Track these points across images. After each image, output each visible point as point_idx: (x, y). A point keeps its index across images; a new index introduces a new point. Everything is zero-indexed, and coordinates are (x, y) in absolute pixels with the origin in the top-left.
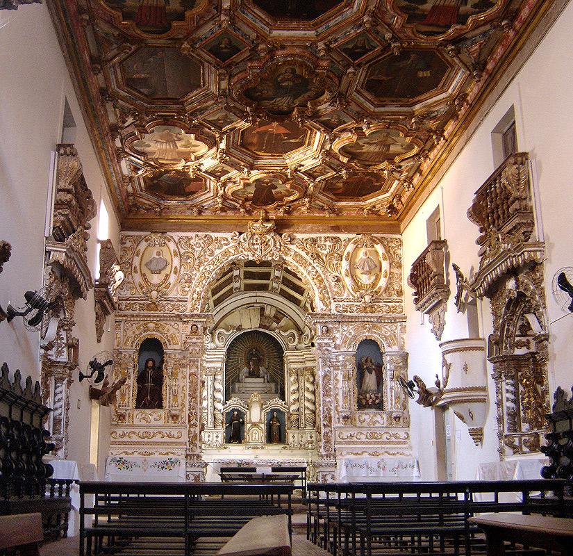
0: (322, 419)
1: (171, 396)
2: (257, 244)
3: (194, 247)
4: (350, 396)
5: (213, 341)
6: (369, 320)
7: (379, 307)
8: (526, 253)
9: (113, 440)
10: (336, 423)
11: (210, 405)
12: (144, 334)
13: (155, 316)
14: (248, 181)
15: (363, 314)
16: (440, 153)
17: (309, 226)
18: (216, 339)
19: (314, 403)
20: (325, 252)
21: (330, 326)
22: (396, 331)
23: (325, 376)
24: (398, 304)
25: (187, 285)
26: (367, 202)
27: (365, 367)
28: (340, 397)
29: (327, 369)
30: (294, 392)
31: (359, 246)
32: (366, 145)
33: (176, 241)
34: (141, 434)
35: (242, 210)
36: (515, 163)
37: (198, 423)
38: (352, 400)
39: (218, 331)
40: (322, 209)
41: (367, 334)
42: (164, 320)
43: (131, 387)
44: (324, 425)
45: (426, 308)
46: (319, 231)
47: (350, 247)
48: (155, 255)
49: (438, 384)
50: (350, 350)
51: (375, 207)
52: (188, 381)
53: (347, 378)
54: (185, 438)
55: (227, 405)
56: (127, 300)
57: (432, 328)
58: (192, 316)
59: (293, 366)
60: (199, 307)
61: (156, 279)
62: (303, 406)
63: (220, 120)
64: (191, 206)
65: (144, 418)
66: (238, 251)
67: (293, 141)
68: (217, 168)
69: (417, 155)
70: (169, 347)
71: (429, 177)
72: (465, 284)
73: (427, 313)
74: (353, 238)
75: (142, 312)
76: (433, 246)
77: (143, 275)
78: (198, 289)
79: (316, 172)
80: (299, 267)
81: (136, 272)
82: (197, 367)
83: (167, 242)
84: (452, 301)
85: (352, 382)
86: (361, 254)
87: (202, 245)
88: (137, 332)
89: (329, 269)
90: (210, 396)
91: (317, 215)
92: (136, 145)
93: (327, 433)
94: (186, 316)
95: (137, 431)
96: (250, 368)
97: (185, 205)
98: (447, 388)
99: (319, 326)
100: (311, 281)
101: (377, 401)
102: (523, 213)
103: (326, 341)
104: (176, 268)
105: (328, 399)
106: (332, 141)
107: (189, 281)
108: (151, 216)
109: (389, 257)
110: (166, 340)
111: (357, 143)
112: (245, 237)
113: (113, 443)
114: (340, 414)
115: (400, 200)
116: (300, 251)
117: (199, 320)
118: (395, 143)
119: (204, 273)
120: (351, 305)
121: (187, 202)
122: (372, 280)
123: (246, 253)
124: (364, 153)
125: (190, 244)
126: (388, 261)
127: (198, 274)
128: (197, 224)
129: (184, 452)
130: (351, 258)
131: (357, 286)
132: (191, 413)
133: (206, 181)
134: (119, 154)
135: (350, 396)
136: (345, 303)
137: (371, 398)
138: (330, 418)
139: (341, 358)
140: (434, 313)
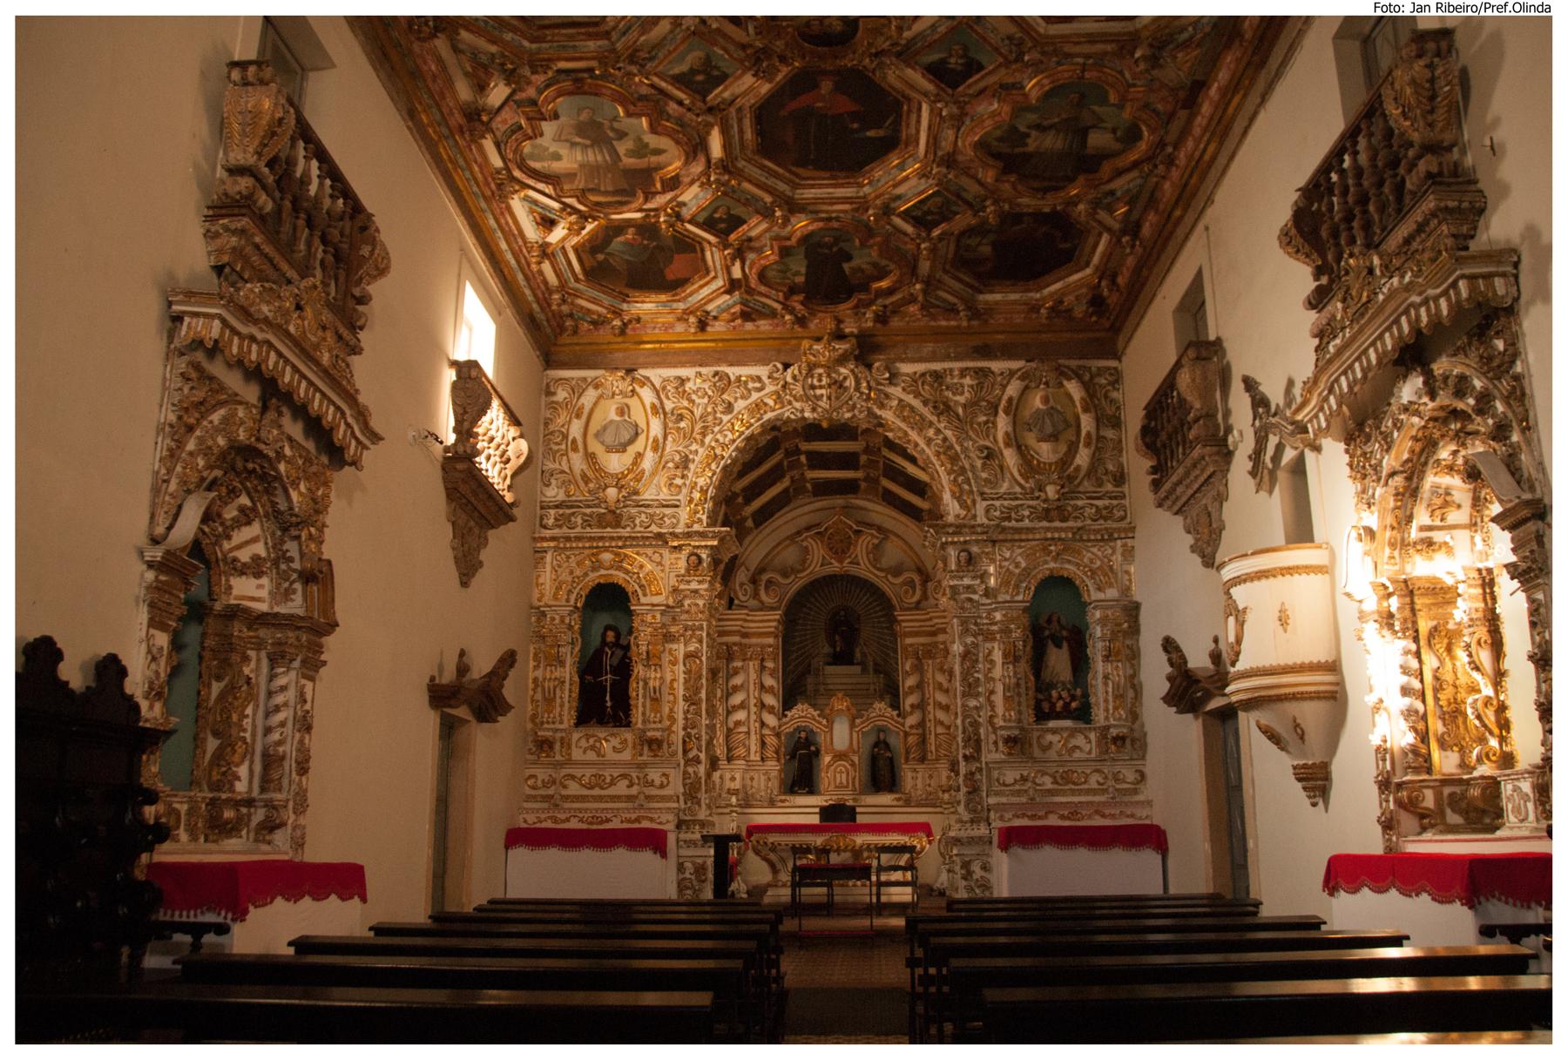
0: (961, 744)
1: (648, 700)
2: (821, 387)
3: (694, 397)
4: (1019, 695)
5: (756, 595)
6: (1056, 535)
7: (1076, 508)
8: (1462, 284)
9: (529, 791)
10: (990, 751)
11: (753, 717)
12: (592, 575)
13: (612, 538)
14: (788, 243)
15: (1045, 524)
16: (1202, 146)
17: (928, 348)
20: (961, 399)
21: (975, 549)
22: (1114, 558)
23: (965, 655)
24: (1115, 502)
25: (679, 473)
26: (1046, 291)
27: (1047, 633)
28: (998, 699)
29: (969, 640)
30: (912, 690)
31: (1033, 385)
32: (1034, 133)
33: (658, 386)
34: (586, 780)
35: (787, 317)
36: (1419, 56)
37: (703, 756)
38: (1024, 704)
39: (765, 577)
40: (951, 310)
41: (1052, 565)
42: (631, 546)
43: (567, 685)
44: (965, 756)
45: (1177, 498)
46: (947, 358)
47: (1013, 389)
48: (613, 416)
49: (1216, 657)
50: (1016, 598)
51: (1061, 302)
52: (682, 668)
53: (1011, 657)
54: (676, 786)
56: (557, 507)
57: (1192, 542)
58: (688, 535)
59: (909, 641)
60: (704, 517)
61: (615, 463)
62: (931, 716)
63: (699, 72)
64: (685, 311)
65: (592, 748)
66: (782, 403)
67: (871, 133)
68: (715, 211)
69: (1149, 158)
70: (643, 600)
71: (1178, 213)
72: (1273, 420)
73: (1176, 513)
74: (1019, 370)
75: (588, 529)
76: (1191, 353)
77: (590, 457)
78: (701, 482)
79: (929, 212)
80: (910, 432)
81: (575, 449)
82: (701, 641)
83: (638, 389)
84: (1241, 464)
85: (1024, 666)
86: (1037, 402)
87: (710, 393)
88: (578, 572)
89: (971, 433)
90: (753, 701)
91: (944, 323)
92: (533, 157)
93: (972, 774)
94: (675, 535)
95: (578, 773)
97: (672, 311)
98: (1240, 666)
99: (952, 552)
100: (934, 459)
101: (1074, 705)
102: (1449, 185)
103: (967, 581)
104: (656, 441)
105: (973, 703)
106: (958, 121)
107: (685, 463)
108: (604, 334)
109: (1095, 406)
110: (637, 587)
111: (1013, 129)
112: (796, 372)
113: (530, 798)
114: (999, 732)
115: (1113, 282)
116: (909, 399)
117: (703, 543)
118: (1097, 125)
119: (713, 448)
120: (1017, 506)
121: (675, 305)
122: (1060, 455)
123: (798, 405)
124: (1027, 157)
125: (685, 391)
126: (1093, 414)
127: (701, 450)
128: (698, 351)
129: (671, 817)
130: (1014, 409)
131: (1030, 466)
132: (689, 735)
133: (703, 251)
134: (502, 186)
135: (1019, 695)
136: (1006, 503)
137: (1060, 697)
138: (978, 741)
139: (998, 616)
140: (1194, 511)
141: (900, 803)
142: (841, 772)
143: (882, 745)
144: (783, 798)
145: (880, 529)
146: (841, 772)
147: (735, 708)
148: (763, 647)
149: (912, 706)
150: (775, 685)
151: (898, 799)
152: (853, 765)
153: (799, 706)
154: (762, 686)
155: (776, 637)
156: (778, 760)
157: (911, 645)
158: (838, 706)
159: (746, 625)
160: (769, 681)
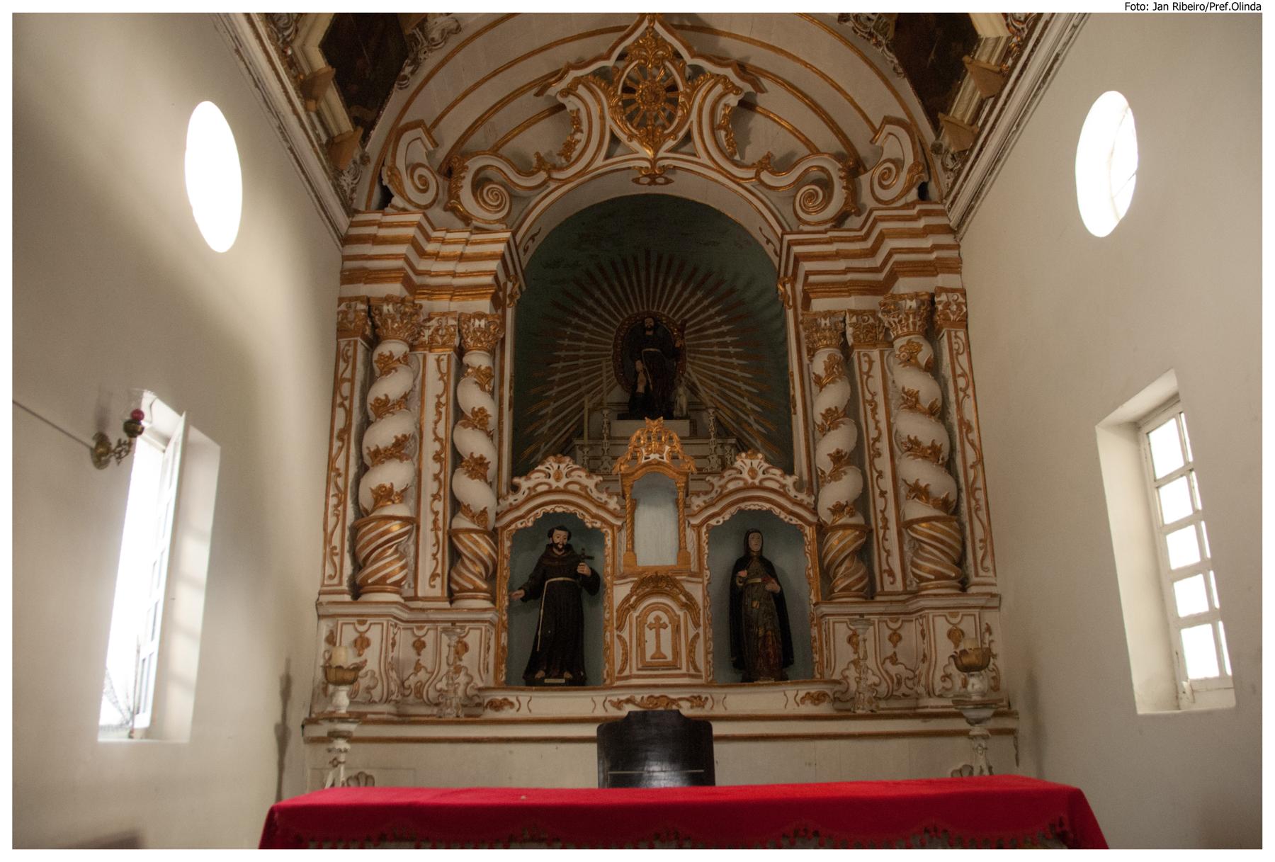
11: (430, 487)
19: (949, 466)
39: (474, 165)
55: (520, 497)
62: (887, 484)
90: (430, 447)
96: (635, 386)
141: (824, 708)
142: (658, 626)
143: (755, 565)
144: (499, 696)
145: (742, 68)
146: (658, 626)
147: (381, 456)
148: (463, 319)
149: (837, 458)
150: (490, 407)
151: (817, 699)
152: (690, 605)
154: (459, 414)
155: (497, 302)
156: (493, 601)
157: (828, 314)
159: (423, 265)
160: (474, 398)
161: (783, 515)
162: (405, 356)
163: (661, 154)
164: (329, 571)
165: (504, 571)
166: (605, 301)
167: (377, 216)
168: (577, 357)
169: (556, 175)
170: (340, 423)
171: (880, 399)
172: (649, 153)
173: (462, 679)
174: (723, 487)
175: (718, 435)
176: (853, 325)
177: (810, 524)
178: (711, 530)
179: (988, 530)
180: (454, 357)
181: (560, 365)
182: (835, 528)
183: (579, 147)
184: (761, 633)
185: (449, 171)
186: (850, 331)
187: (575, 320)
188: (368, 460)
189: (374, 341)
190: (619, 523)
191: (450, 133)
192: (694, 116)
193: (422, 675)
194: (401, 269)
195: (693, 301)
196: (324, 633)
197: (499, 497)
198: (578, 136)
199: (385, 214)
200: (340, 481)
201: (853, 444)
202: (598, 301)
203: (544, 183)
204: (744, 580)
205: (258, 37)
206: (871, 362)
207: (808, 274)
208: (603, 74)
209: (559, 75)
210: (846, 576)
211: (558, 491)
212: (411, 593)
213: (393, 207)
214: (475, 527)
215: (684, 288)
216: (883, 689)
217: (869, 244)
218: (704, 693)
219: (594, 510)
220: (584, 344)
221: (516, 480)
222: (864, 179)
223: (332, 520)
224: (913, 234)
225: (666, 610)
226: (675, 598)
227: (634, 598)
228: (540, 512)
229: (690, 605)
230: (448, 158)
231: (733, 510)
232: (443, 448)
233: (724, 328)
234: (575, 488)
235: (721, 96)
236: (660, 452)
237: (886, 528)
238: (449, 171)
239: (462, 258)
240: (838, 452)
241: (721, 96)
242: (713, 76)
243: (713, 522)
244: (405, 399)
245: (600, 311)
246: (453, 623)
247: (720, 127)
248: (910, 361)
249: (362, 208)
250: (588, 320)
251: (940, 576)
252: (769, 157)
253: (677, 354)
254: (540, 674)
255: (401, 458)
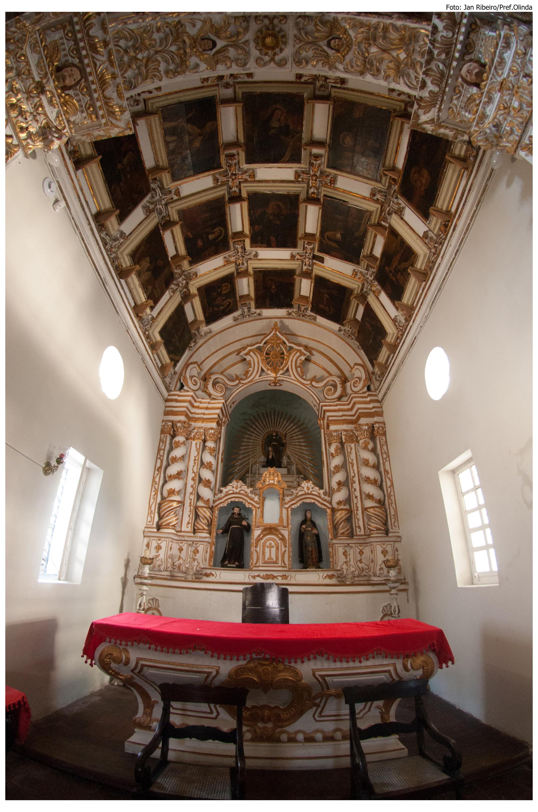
11: (189, 490)
18: (210, 387)
30: (338, 469)
39: (213, 377)
55: (223, 495)
62: (357, 493)
90: (191, 475)
96: (268, 456)
141: (334, 581)
142: (271, 547)
143: (309, 523)
145: (306, 347)
146: (271, 547)
147: (171, 477)
149: (339, 483)
150: (214, 462)
151: (331, 577)
152: (283, 539)
153: (234, 483)
154: (202, 463)
155: (218, 424)
156: (210, 534)
157: (336, 431)
158: (269, 481)
159: (193, 410)
160: (208, 458)
161: (319, 505)
162: (184, 442)
163: (278, 375)
164: (149, 519)
165: (215, 522)
166: (259, 426)
167: (178, 393)
168: (249, 445)
169: (242, 382)
170: (158, 465)
171: (355, 462)
172: (273, 375)
173: (196, 563)
174: (297, 493)
175: (297, 474)
176: (345, 435)
177: (329, 508)
178: (292, 509)
179: (396, 511)
180: (202, 443)
181: (243, 448)
182: (338, 510)
183: (250, 373)
184: (310, 549)
185: (205, 379)
186: (343, 437)
187: (249, 433)
188: (167, 479)
189: (173, 436)
190: (258, 506)
191: (206, 367)
192: (289, 363)
193: (181, 561)
194: (185, 411)
195: (289, 427)
196: (146, 543)
197: (215, 495)
198: (250, 369)
199: (180, 392)
200: (156, 486)
201: (345, 478)
202: (257, 426)
203: (238, 384)
204: (304, 529)
205: (135, 327)
206: (351, 449)
207: (328, 417)
208: (259, 348)
209: (244, 348)
210: (343, 529)
211: (236, 493)
212: (179, 529)
213: (184, 390)
214: (205, 505)
215: (287, 422)
216: (356, 573)
217: (350, 407)
218: (287, 574)
219: (249, 501)
220: (252, 441)
221: (222, 489)
222: (348, 384)
223: (152, 500)
224: (366, 403)
225: (274, 540)
226: (277, 536)
227: (262, 535)
228: (229, 501)
229: (283, 539)
230: (205, 375)
231: (301, 502)
232: (195, 476)
233: (300, 437)
234: (243, 492)
235: (299, 357)
236: (274, 480)
237: (357, 510)
238: (205, 379)
239: (207, 408)
240: (340, 481)
241: (299, 357)
242: (296, 350)
243: (293, 507)
244: (183, 457)
245: (257, 429)
246: (193, 542)
247: (298, 367)
248: (365, 448)
249: (173, 390)
250: (253, 433)
251: (378, 529)
252: (315, 377)
253: (284, 445)
254: (226, 562)
255: (179, 479)
